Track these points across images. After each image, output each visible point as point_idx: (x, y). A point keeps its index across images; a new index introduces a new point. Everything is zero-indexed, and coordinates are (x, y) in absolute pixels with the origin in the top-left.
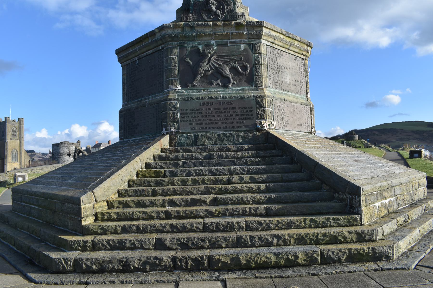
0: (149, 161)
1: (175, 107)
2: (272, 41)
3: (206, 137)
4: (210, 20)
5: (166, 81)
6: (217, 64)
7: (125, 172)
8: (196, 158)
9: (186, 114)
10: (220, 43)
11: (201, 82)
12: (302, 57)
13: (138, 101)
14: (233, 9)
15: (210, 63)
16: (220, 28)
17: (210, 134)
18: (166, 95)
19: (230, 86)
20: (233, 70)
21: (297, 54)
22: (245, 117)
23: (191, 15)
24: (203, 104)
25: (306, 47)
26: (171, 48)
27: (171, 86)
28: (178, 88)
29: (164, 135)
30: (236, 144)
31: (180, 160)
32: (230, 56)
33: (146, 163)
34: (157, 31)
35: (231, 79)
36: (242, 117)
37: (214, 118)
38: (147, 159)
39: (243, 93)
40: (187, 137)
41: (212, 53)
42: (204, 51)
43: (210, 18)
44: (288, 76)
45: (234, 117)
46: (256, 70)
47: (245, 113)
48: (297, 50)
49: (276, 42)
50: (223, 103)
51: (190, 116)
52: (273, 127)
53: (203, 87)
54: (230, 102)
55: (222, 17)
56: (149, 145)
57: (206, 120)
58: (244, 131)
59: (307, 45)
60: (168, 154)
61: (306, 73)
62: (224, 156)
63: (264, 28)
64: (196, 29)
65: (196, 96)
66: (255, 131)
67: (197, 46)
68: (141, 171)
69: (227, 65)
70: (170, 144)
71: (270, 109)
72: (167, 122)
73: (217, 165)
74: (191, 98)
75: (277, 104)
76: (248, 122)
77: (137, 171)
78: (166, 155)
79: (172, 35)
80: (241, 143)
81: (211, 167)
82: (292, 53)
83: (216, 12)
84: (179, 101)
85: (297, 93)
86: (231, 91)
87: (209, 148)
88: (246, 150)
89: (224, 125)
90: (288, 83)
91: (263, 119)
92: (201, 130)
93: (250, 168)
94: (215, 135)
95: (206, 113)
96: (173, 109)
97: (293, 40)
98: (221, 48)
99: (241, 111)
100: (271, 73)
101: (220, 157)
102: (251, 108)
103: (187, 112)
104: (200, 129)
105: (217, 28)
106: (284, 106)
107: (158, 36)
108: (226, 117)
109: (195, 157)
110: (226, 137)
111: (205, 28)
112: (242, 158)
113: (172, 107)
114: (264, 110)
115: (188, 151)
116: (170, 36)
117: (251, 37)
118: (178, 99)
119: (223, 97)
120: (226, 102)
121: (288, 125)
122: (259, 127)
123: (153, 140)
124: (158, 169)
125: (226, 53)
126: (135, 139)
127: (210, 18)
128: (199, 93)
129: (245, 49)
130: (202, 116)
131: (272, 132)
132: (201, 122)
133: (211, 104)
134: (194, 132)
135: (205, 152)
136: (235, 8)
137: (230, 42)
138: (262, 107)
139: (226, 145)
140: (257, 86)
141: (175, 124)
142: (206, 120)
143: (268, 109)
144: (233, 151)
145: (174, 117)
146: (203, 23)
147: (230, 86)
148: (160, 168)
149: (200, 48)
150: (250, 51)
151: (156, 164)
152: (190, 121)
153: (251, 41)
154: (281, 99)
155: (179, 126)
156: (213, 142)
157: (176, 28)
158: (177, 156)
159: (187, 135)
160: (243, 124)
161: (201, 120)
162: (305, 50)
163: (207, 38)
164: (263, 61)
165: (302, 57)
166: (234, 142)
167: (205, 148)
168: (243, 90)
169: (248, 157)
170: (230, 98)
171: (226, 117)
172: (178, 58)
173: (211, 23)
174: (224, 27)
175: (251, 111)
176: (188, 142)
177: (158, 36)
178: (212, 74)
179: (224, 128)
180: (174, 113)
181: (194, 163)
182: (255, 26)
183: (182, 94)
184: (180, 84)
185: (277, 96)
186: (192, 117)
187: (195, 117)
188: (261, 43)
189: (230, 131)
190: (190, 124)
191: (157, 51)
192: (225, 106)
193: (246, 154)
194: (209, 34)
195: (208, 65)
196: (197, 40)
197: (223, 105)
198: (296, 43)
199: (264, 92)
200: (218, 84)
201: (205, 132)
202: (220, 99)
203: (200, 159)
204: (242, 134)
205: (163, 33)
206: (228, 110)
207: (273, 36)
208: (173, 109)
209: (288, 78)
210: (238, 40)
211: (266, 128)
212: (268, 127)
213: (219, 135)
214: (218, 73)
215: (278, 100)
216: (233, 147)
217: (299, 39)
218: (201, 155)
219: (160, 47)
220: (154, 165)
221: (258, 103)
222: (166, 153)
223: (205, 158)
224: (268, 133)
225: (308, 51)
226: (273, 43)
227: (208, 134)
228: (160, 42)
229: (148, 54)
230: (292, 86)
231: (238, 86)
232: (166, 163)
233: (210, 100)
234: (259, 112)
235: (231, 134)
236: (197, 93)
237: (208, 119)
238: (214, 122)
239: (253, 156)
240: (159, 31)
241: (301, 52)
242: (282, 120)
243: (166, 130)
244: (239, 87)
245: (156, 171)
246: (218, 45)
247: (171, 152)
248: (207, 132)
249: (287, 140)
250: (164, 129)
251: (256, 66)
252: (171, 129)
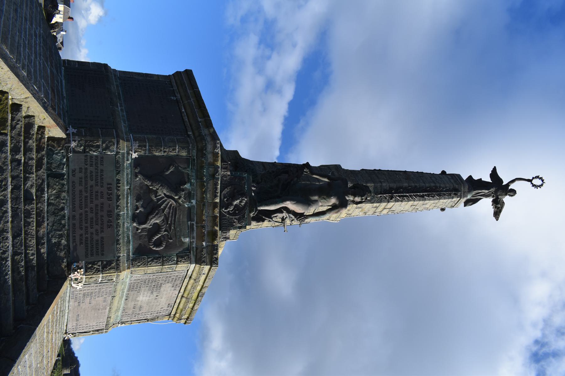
0: (24, 109)
1: (107, 148)
2: (193, 277)
3: (61, 191)
4: (222, 197)
5: (144, 137)
6: (165, 208)
7: (5, 77)
8: (26, 179)
9: (96, 163)
10: (192, 211)
11: (142, 186)
12: (173, 313)
13: (119, 94)
14: (234, 225)
15: (166, 198)
16: (211, 212)
17: (64, 197)
18: (125, 136)
19: (135, 224)
20: (156, 228)
21: (176, 306)
22: (89, 245)
23: (229, 173)
24: (110, 187)
25: (185, 316)
26: (188, 147)
27: (137, 145)
28: (133, 154)
29: (65, 130)
30: (48, 234)
31: (25, 155)
32: (174, 224)
33: (21, 105)
34: (212, 130)
35: (143, 226)
36: (89, 242)
37: (89, 202)
38: (28, 108)
39: (123, 242)
40: (61, 164)
41: (180, 201)
42: (183, 190)
43: (224, 198)
44: (148, 298)
45: (90, 230)
46: (155, 258)
47: (94, 246)
48: (181, 306)
49: (192, 281)
50: (109, 216)
51: (92, 169)
52: (73, 285)
53: (134, 188)
54: (111, 225)
55: (225, 212)
56: (50, 109)
57: (86, 192)
58: (68, 245)
59: (188, 318)
60: (35, 137)
61: (152, 319)
62: (28, 220)
63: (208, 267)
64: (211, 181)
65: (121, 179)
66: (67, 261)
67: (189, 181)
68: (7, 98)
69: (163, 220)
70: (51, 139)
71: (100, 279)
72: (86, 136)
73: (14, 210)
74: (120, 171)
75: (107, 288)
76: (81, 250)
77: (7, 93)
78: (33, 134)
79: (205, 150)
80: (49, 241)
81: (11, 201)
82: (178, 301)
83: (232, 205)
84: (116, 155)
85: (124, 310)
86: (127, 226)
87: (42, 197)
88: (38, 250)
89: (77, 217)
90: (138, 299)
91: (86, 271)
92: (71, 184)
93: (7, 261)
94: (63, 203)
95: (97, 192)
96: (104, 145)
97: (194, 302)
98: (186, 212)
99: (97, 241)
100: (151, 277)
101: (28, 214)
102: (103, 254)
103: (99, 165)
104: (73, 182)
105: (211, 208)
106: (105, 296)
108: (89, 220)
109: (29, 178)
110: (60, 220)
111: (211, 192)
112: (25, 246)
113: (107, 145)
114: (99, 271)
115: (39, 165)
116: (204, 148)
117: (198, 251)
118: (118, 153)
119: (118, 215)
120: (112, 219)
121: (77, 304)
122: (74, 266)
123: (59, 115)
124: (9, 122)
125: (179, 218)
126: (64, 84)
127: (224, 198)
128: (125, 183)
129: (183, 243)
130: (92, 186)
131: (67, 284)
132: (83, 184)
133: (109, 199)
134: (68, 174)
135: (37, 191)
136: (235, 228)
137: (193, 224)
138: (103, 268)
139: (48, 220)
140: (133, 260)
141: (82, 148)
142: (86, 192)
143: (100, 277)
144: (37, 231)
145: (93, 146)
146: (219, 191)
147: (135, 224)
148: (11, 125)
149: (187, 186)
150: (181, 250)
151: (19, 120)
152: (86, 169)
153: (193, 251)
154: (115, 292)
155: (79, 152)
156: (52, 201)
157: (214, 157)
158: (31, 150)
159: (64, 164)
160: (78, 244)
161: (86, 184)
162: (181, 315)
163: (199, 195)
164: (167, 266)
165: (173, 313)
166: (51, 232)
167: (42, 191)
168: (129, 242)
169: (26, 254)
170: (118, 225)
171: (89, 220)
172: (174, 156)
173: (218, 200)
174: (212, 217)
175: (97, 254)
176: (54, 165)
177: (205, 132)
178: (152, 200)
179: (74, 216)
180: (98, 147)
181: (18, 176)
182: (212, 256)
183: (126, 159)
184: (140, 156)
185: (119, 287)
186: (91, 172)
187: (91, 176)
188: (191, 263)
189: (69, 226)
190: (81, 169)
191: (186, 127)
192: (106, 219)
193: (32, 251)
194: (204, 197)
195: (163, 195)
197: (108, 215)
198: (191, 305)
199: (124, 270)
200: (137, 208)
201: (68, 189)
202: (116, 211)
203: (25, 185)
204: (64, 242)
205: (209, 139)
206: (100, 222)
207: (199, 278)
208: (104, 145)
209: (144, 298)
210: (195, 235)
211: (72, 276)
212: (73, 278)
213: (63, 209)
214: (152, 208)
215: (113, 289)
216: (43, 231)
217: (195, 308)
218: (32, 186)
219: (190, 133)
220: (17, 117)
221: (109, 263)
222: (37, 133)
223: (27, 193)
224: (65, 279)
225: (180, 319)
226: (190, 277)
227: (64, 194)
228: (197, 134)
229: (183, 115)
230: (133, 303)
231: (135, 235)
232: (19, 135)
233: (115, 197)
234: (95, 264)
235: (64, 226)
236: (125, 179)
237: (88, 194)
238: (83, 203)
239: (28, 261)
240: (210, 134)
241: (179, 311)
242: (84, 295)
243: (73, 133)
244: (133, 236)
245: (7, 121)
246: (189, 208)
247: (39, 140)
248: (68, 192)
249: (54, 308)
250: (75, 131)
251: (161, 258)
252: (75, 141)
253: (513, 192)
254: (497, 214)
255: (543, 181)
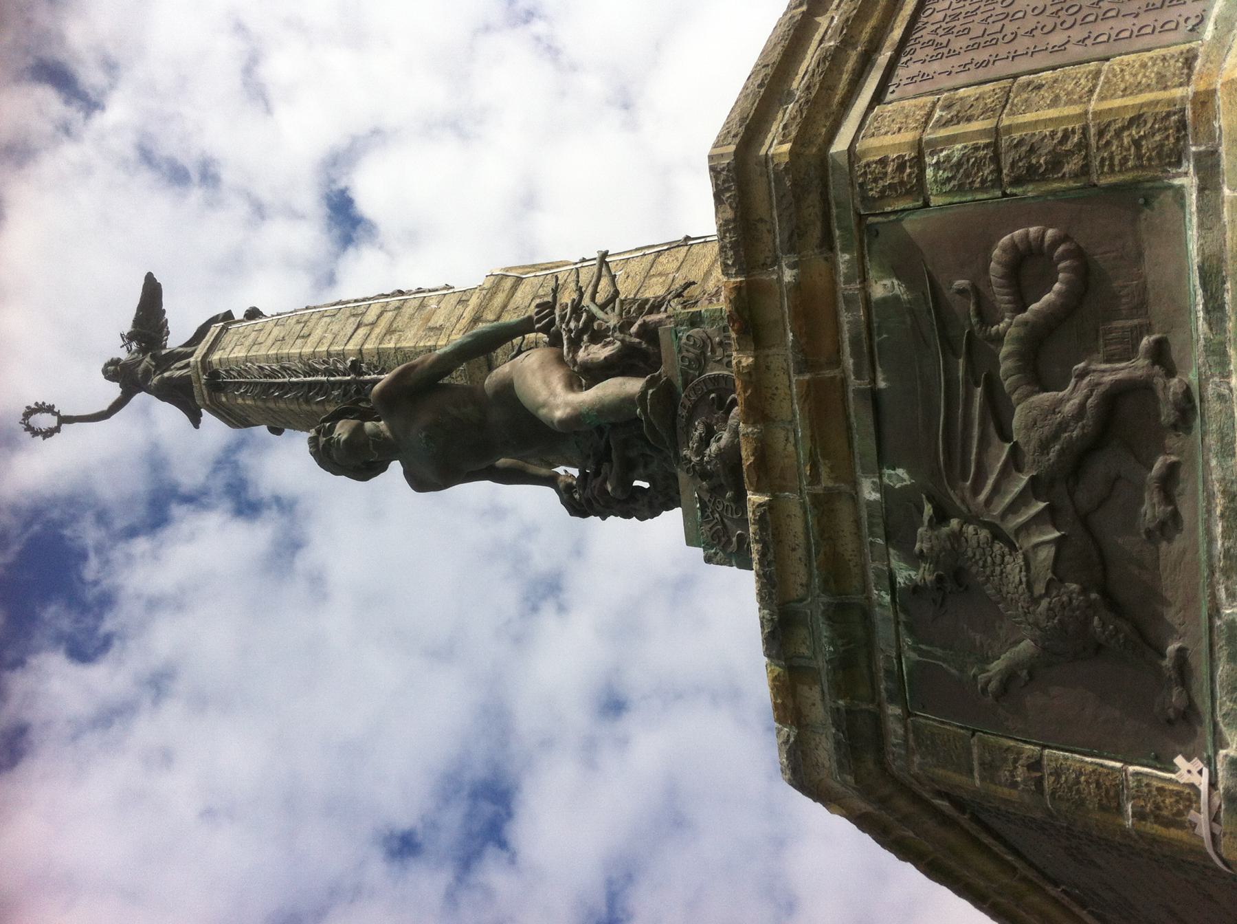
20: (1043, 359)
35: (1122, 371)
107: (864, 807)
117: (816, 233)
164: (976, 126)
173: (754, 498)
196: (865, 589)
210: (845, 318)
244: (1185, 311)
253: (114, 371)
254: (152, 292)
255: (29, 428)
